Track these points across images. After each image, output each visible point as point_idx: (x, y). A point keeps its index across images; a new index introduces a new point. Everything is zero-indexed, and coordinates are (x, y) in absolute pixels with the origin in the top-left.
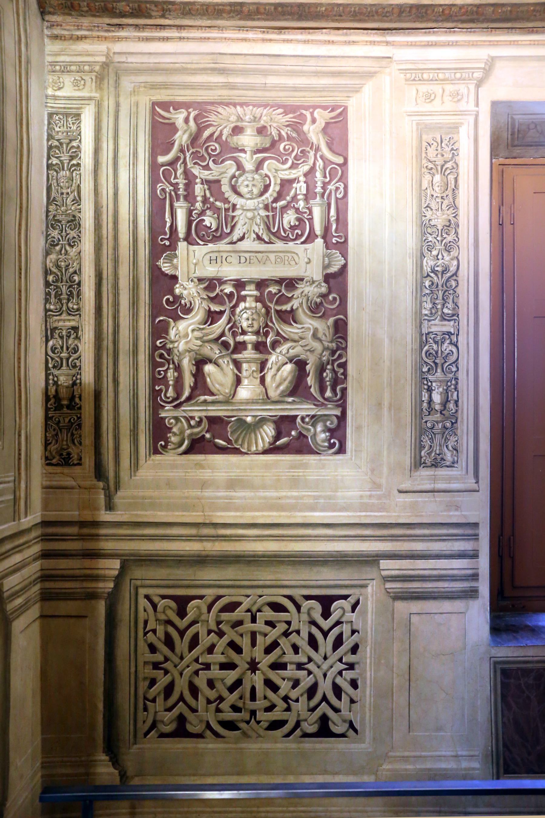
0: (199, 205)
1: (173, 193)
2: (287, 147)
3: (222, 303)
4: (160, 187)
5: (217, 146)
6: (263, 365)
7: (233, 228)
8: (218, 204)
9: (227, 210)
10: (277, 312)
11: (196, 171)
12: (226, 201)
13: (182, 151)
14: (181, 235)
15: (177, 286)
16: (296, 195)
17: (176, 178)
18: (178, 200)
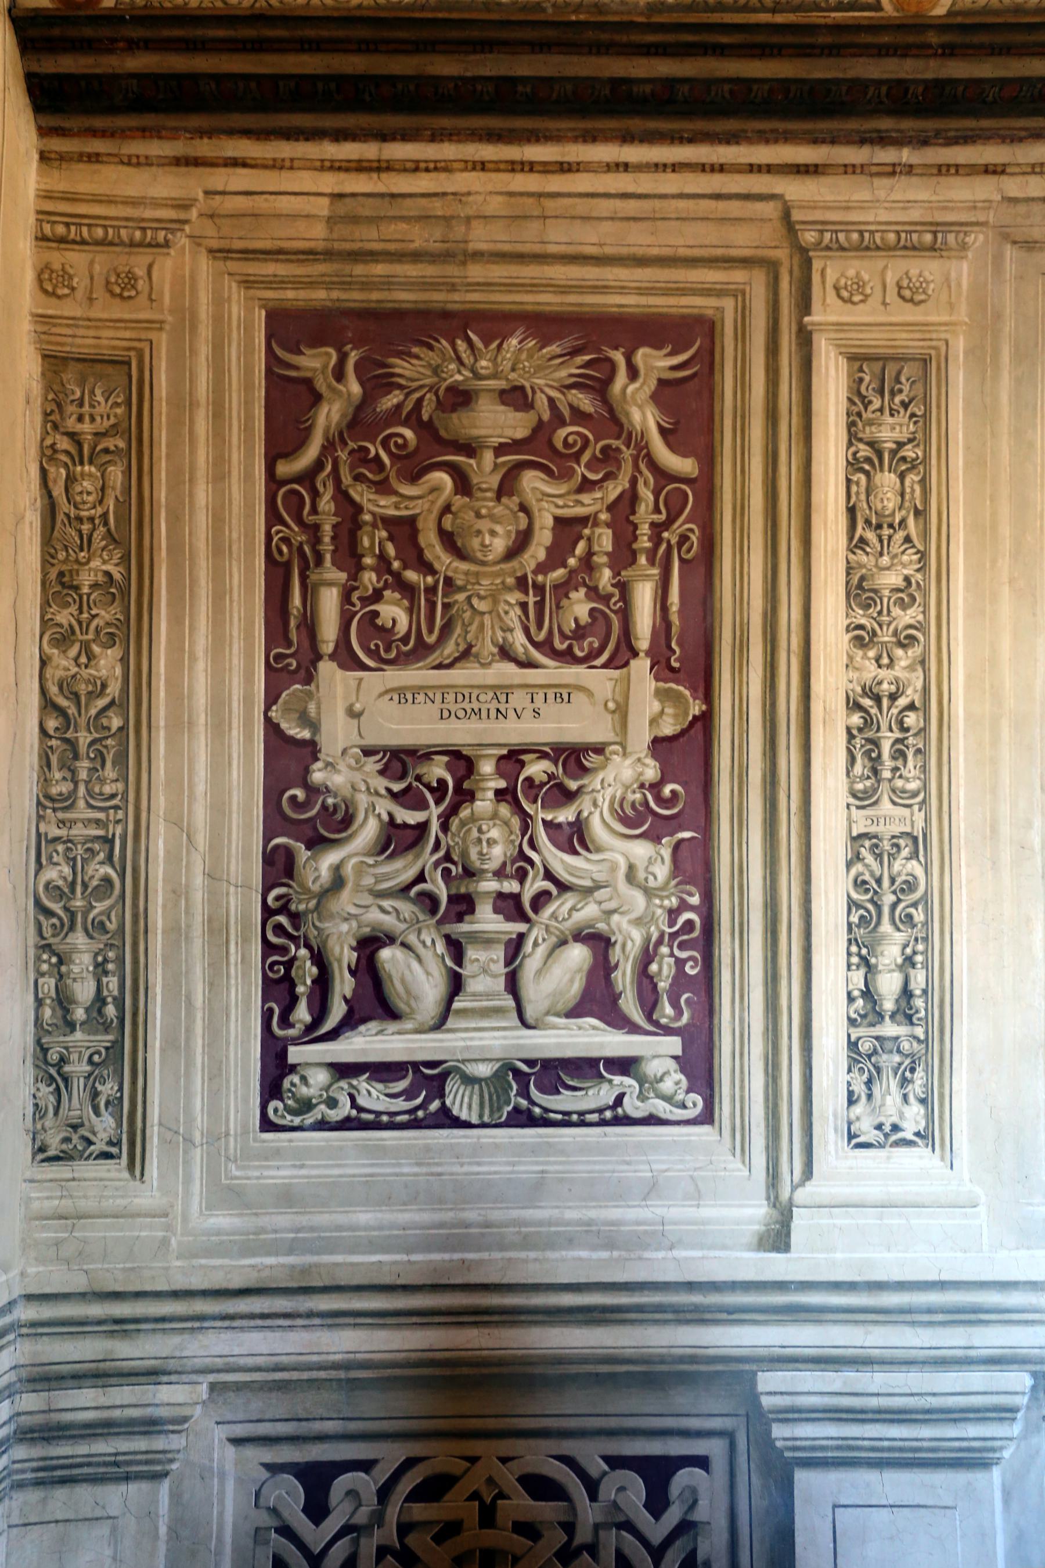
0: (370, 579)
1: (307, 549)
2: (571, 440)
3: (422, 805)
4: (278, 532)
5: (408, 433)
6: (515, 947)
7: (447, 629)
8: (411, 576)
9: (431, 590)
10: (547, 824)
11: (361, 494)
12: (428, 568)
13: (328, 447)
14: (328, 648)
15: (319, 765)
16: (590, 554)
17: (314, 510)
18: (319, 560)
